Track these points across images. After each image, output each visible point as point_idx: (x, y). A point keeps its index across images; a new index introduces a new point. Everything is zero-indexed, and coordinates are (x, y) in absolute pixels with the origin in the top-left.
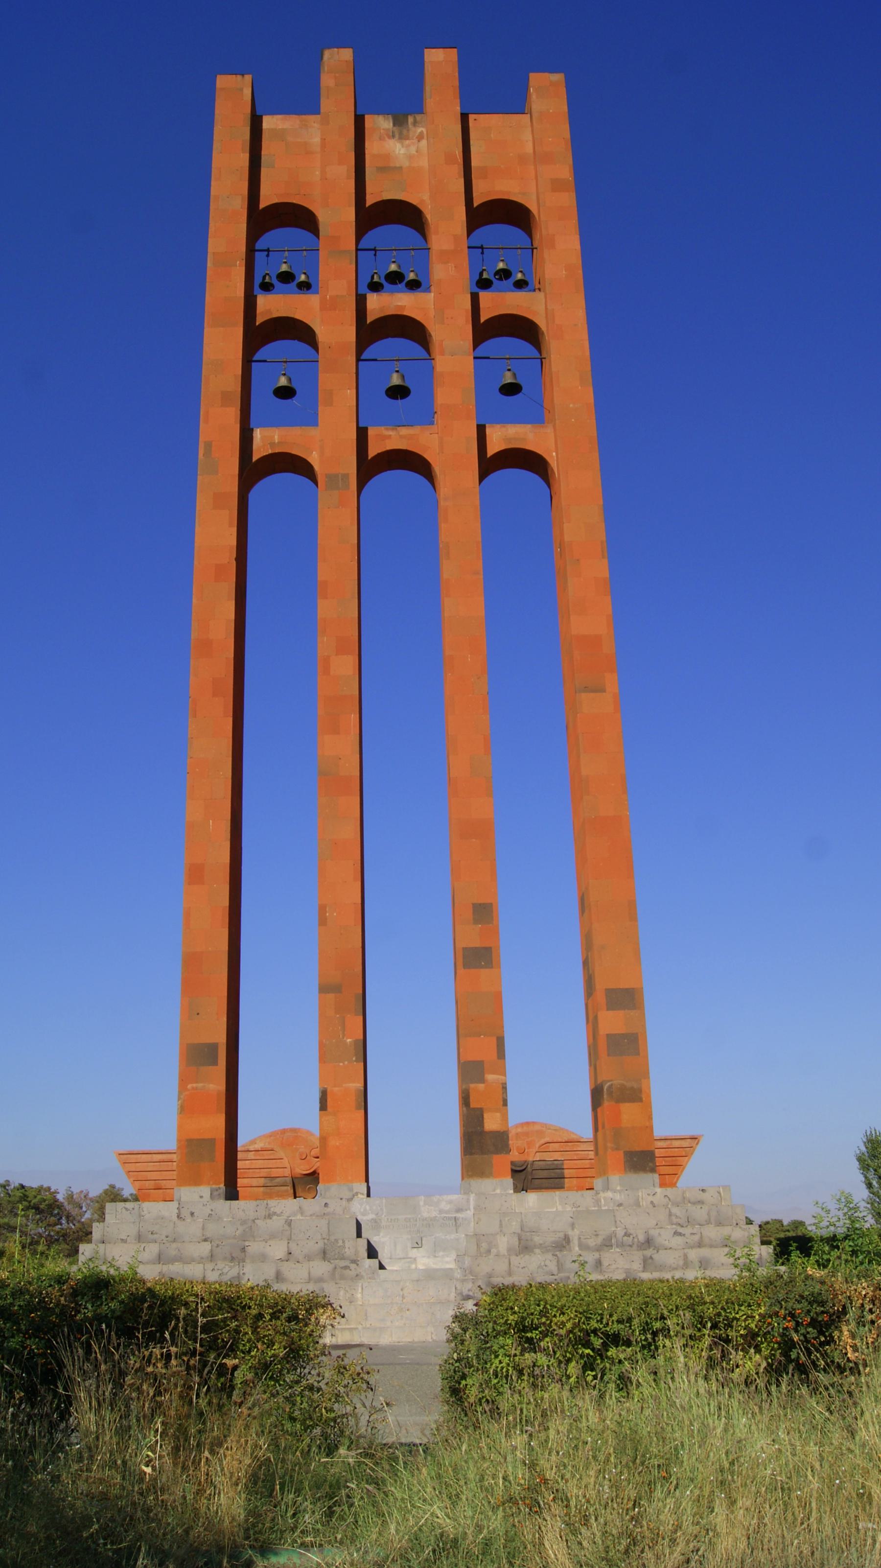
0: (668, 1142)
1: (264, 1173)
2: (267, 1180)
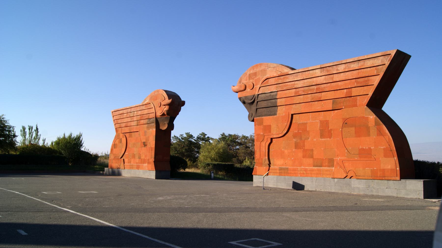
0: (361, 63)
2: (147, 120)
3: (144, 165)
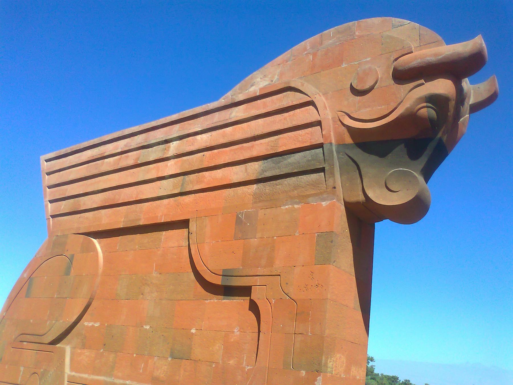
1: (260, 148)
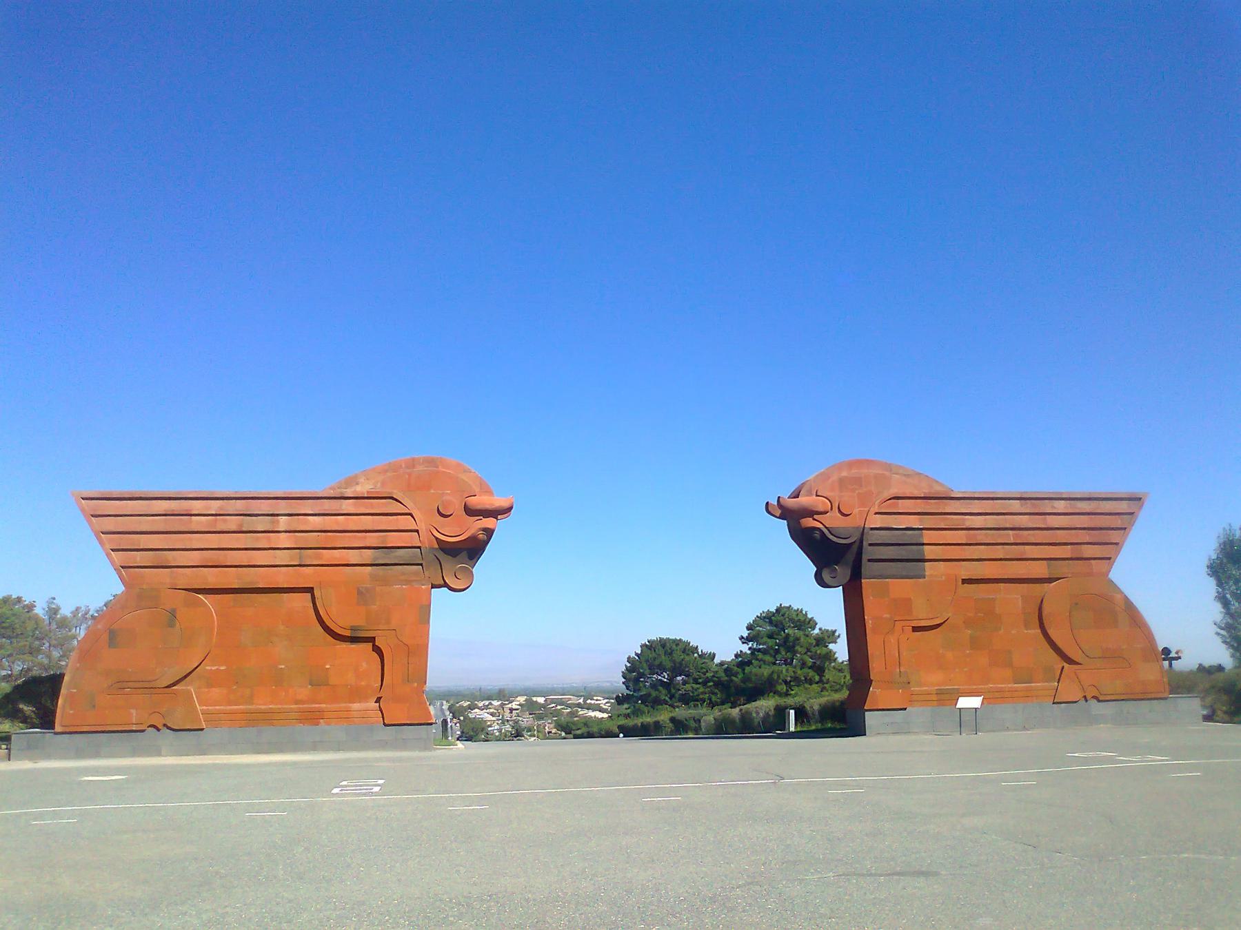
1: (372, 540)
3: (356, 706)
